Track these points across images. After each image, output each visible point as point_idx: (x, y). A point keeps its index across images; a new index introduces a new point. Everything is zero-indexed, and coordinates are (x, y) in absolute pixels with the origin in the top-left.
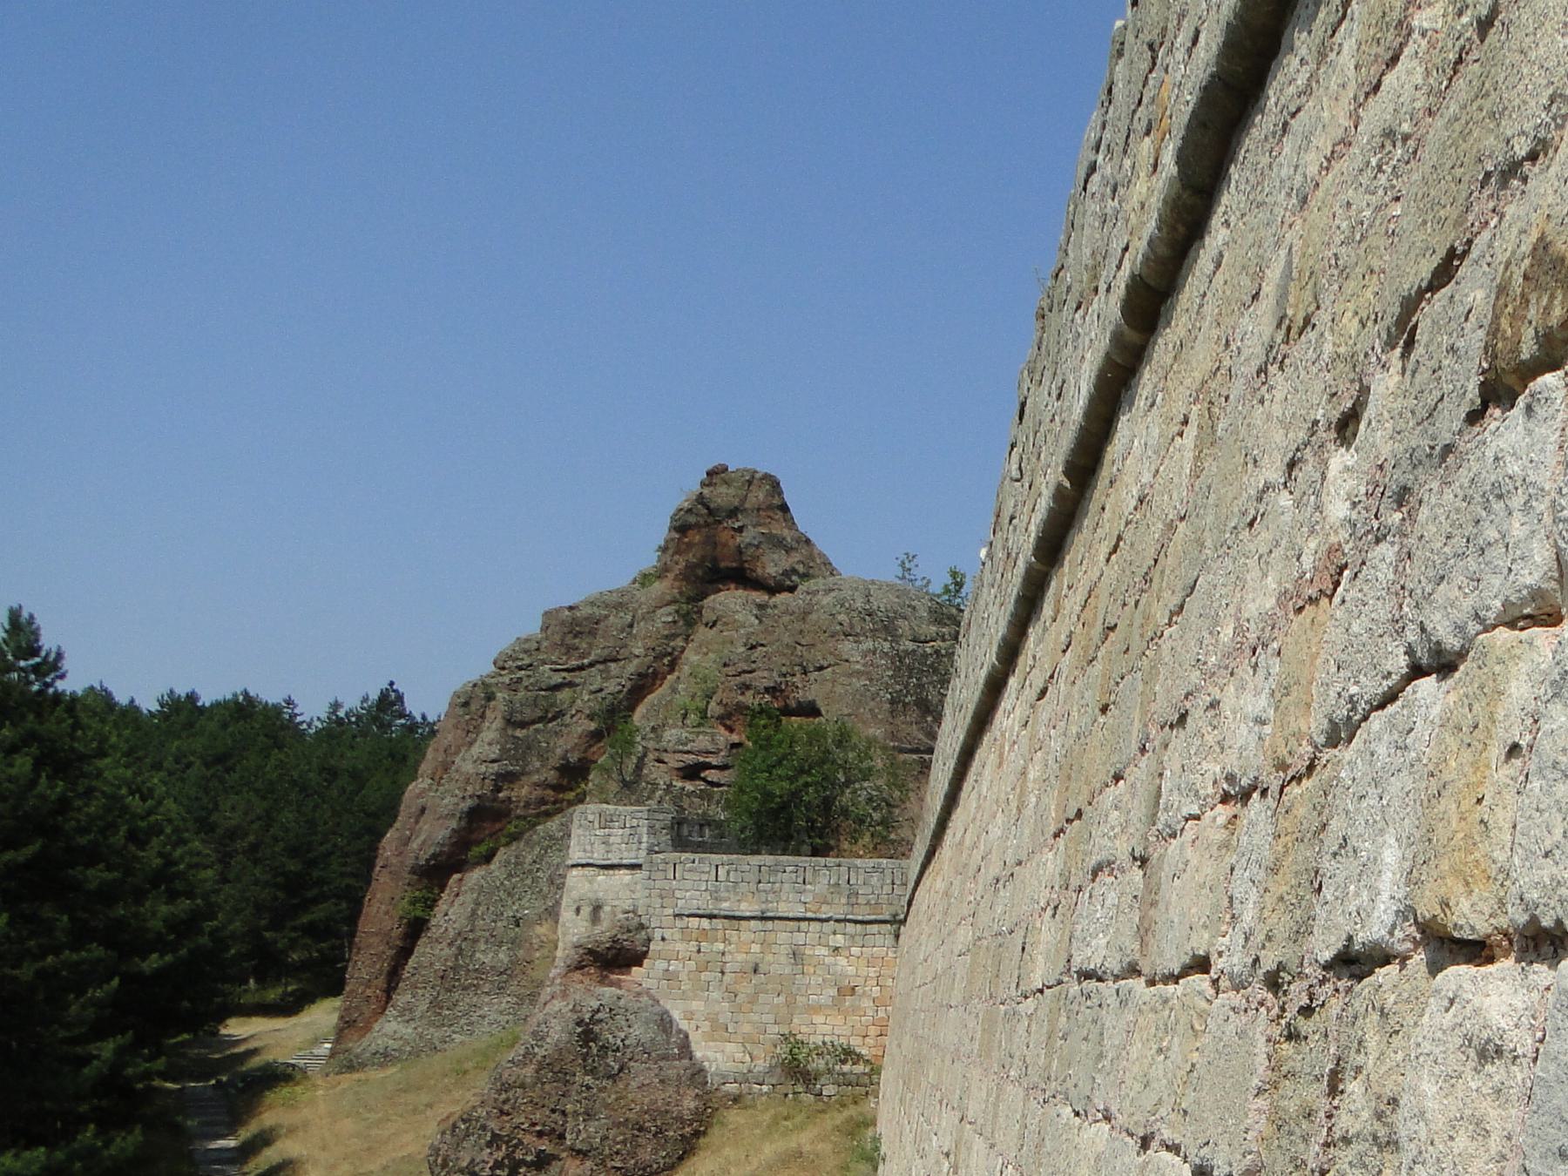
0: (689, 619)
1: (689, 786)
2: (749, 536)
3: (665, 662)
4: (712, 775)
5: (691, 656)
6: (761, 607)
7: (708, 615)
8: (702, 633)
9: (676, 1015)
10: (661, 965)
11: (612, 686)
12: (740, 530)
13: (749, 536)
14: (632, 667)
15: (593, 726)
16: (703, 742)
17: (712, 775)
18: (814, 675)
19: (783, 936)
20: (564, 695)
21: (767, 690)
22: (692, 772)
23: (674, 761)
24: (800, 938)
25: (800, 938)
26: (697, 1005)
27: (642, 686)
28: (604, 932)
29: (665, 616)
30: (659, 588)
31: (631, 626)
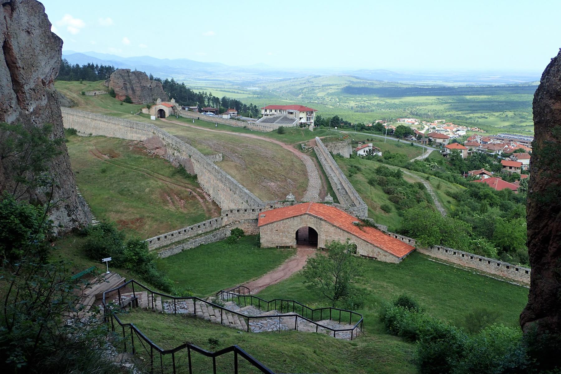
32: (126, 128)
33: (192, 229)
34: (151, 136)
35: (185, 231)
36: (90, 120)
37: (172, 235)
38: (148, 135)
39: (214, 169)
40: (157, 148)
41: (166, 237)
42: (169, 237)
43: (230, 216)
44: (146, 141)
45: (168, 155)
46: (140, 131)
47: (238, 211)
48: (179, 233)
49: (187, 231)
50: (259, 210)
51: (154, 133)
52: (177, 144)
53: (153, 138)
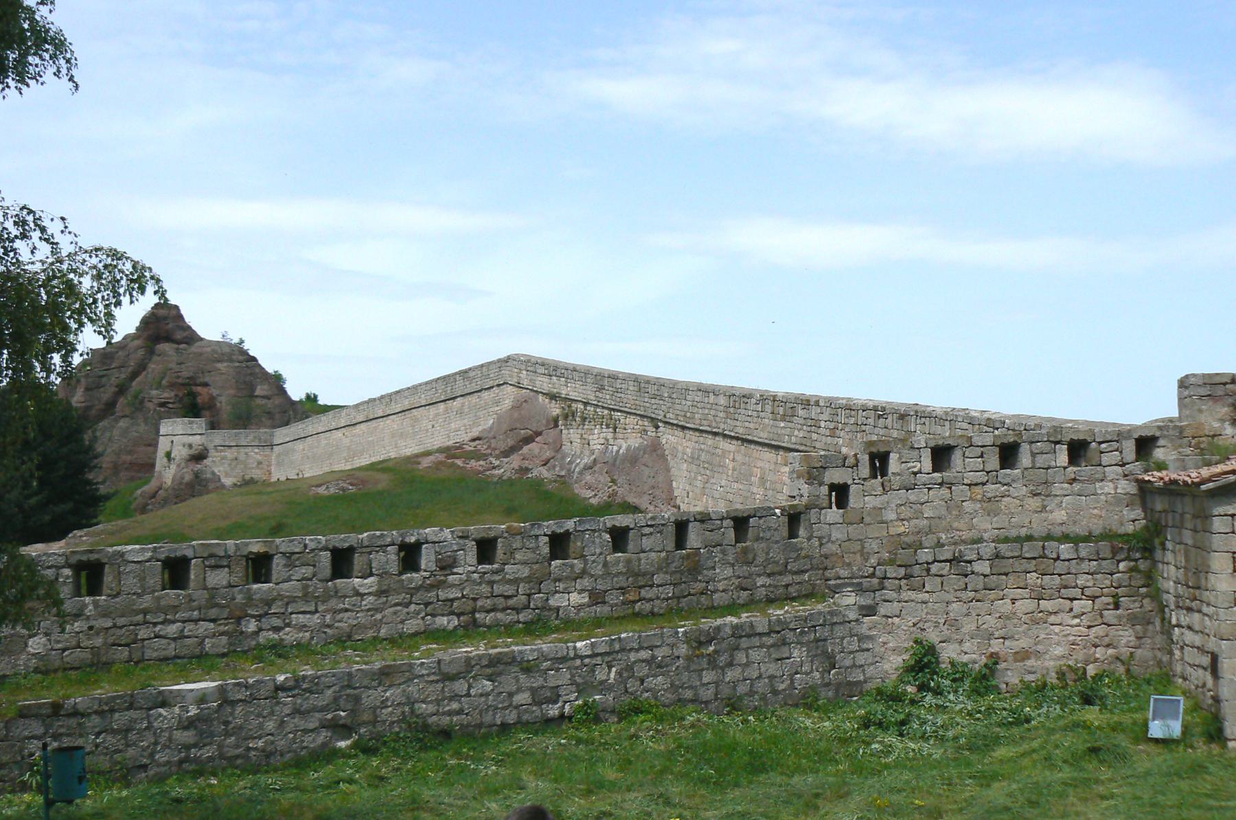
0: (151, 352)
1: (162, 410)
2: (170, 326)
3: (141, 367)
4: (170, 406)
5: (152, 366)
6: (178, 349)
7: (157, 352)
8: (155, 358)
9: (216, 471)
10: (211, 459)
11: (123, 376)
12: (168, 324)
13: (170, 326)
14: (130, 369)
15: (117, 389)
16: (166, 395)
17: (170, 406)
18: (207, 374)
19: (242, 450)
20: (104, 380)
21: (188, 378)
22: (163, 405)
23: (156, 401)
24: (247, 450)
25: (247, 450)
26: (221, 469)
27: (134, 375)
28: (192, 452)
29: (141, 352)
30: (137, 343)
31: (128, 355)
32: (433, 410)
33: (486, 549)
34: (507, 403)
35: (410, 555)
36: (339, 434)
37: (259, 566)
38: (497, 403)
39: (768, 408)
40: (528, 440)
41: (176, 571)
42: (218, 578)
43: (871, 502)
44: (491, 428)
45: (563, 458)
46: (473, 399)
47: (941, 455)
48: (342, 562)
49: (427, 559)
50: (1129, 448)
51: (518, 386)
52: (601, 388)
53: (517, 407)
